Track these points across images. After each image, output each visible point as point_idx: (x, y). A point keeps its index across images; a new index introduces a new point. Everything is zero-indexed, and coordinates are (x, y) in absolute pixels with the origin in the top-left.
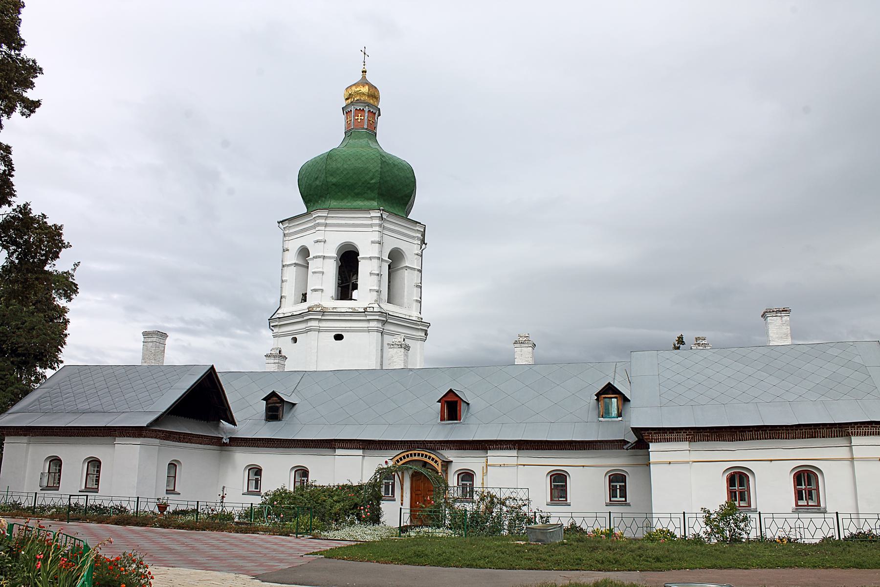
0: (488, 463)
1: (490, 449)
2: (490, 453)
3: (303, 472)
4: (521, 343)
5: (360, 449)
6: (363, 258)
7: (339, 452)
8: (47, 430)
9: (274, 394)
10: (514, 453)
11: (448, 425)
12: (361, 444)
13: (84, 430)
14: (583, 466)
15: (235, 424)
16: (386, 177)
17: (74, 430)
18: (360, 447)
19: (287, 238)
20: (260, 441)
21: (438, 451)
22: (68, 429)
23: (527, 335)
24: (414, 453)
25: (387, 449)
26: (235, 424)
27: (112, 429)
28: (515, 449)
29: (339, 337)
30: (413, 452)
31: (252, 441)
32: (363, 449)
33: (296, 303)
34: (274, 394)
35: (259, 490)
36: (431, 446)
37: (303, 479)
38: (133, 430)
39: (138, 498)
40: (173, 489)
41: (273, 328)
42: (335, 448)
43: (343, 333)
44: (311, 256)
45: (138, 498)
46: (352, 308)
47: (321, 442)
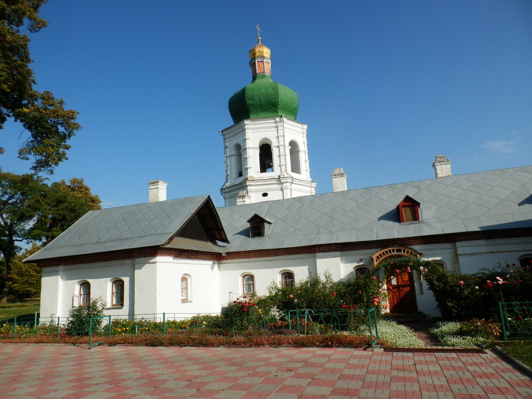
0: (459, 252)
1: (458, 241)
2: (458, 244)
3: (288, 276)
4: (440, 162)
5: (337, 251)
6: (274, 146)
7: (318, 254)
8: (75, 259)
9: (256, 217)
10: (483, 242)
11: (411, 225)
12: (338, 246)
13: (107, 255)
14: (493, 253)
15: (228, 242)
16: (282, 98)
17: (98, 256)
18: (337, 249)
19: (227, 140)
20: (250, 253)
21: (410, 247)
22: (93, 256)
23: (443, 156)
24: (389, 250)
25: (360, 249)
26: (228, 242)
27: (130, 252)
28: (483, 239)
29: (265, 195)
30: (387, 249)
31: (244, 254)
32: (340, 251)
33: (236, 178)
34: (256, 217)
35: (252, 292)
36: (401, 243)
37: (286, 280)
38: (150, 250)
39: (164, 314)
40: (185, 298)
41: (223, 195)
42: (315, 252)
43: (267, 192)
44: (242, 149)
45: (164, 314)
46: (271, 177)
47: (302, 249)
